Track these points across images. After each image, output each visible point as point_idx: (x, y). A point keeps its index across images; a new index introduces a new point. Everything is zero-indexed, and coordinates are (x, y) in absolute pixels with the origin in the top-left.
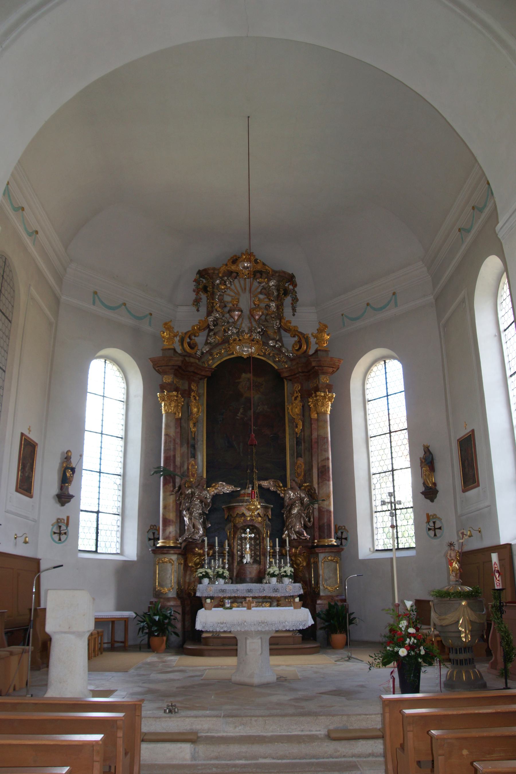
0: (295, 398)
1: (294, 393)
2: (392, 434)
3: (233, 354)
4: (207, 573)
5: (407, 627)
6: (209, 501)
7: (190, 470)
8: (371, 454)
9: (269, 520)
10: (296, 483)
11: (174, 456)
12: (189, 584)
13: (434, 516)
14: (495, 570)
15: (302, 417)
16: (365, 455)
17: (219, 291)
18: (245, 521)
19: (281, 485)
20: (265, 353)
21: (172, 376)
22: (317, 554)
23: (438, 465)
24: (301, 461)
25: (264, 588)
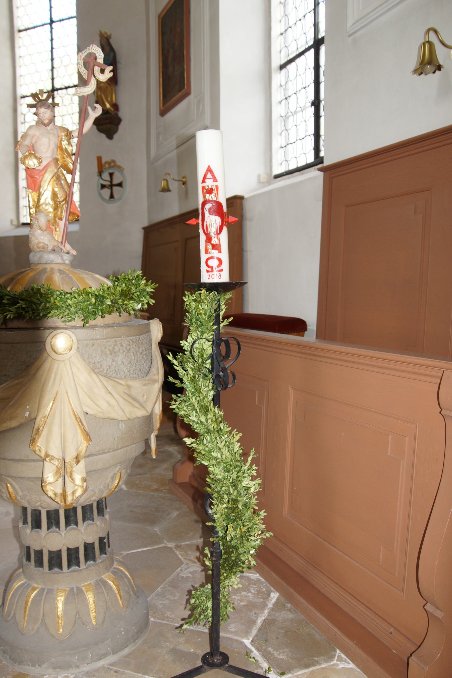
13: (112, 164)
14: (204, 203)
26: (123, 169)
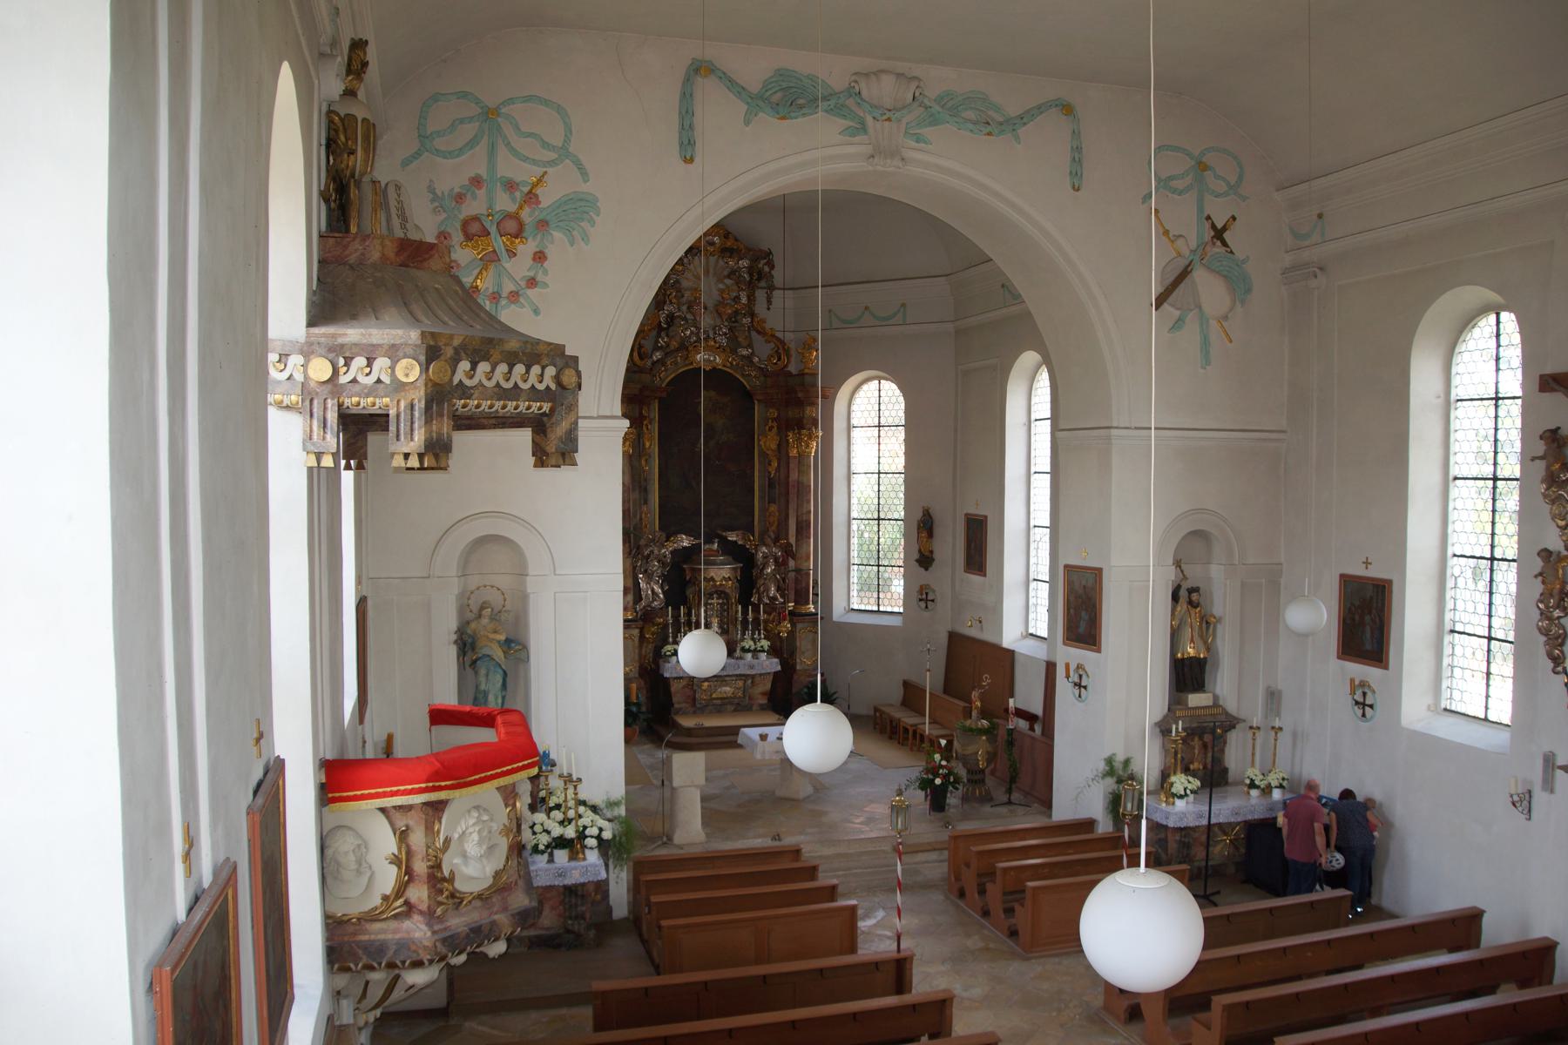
3: (692, 363)
13: (927, 586)
16: (846, 496)
18: (715, 586)
20: (731, 363)
23: (937, 531)
24: (773, 508)
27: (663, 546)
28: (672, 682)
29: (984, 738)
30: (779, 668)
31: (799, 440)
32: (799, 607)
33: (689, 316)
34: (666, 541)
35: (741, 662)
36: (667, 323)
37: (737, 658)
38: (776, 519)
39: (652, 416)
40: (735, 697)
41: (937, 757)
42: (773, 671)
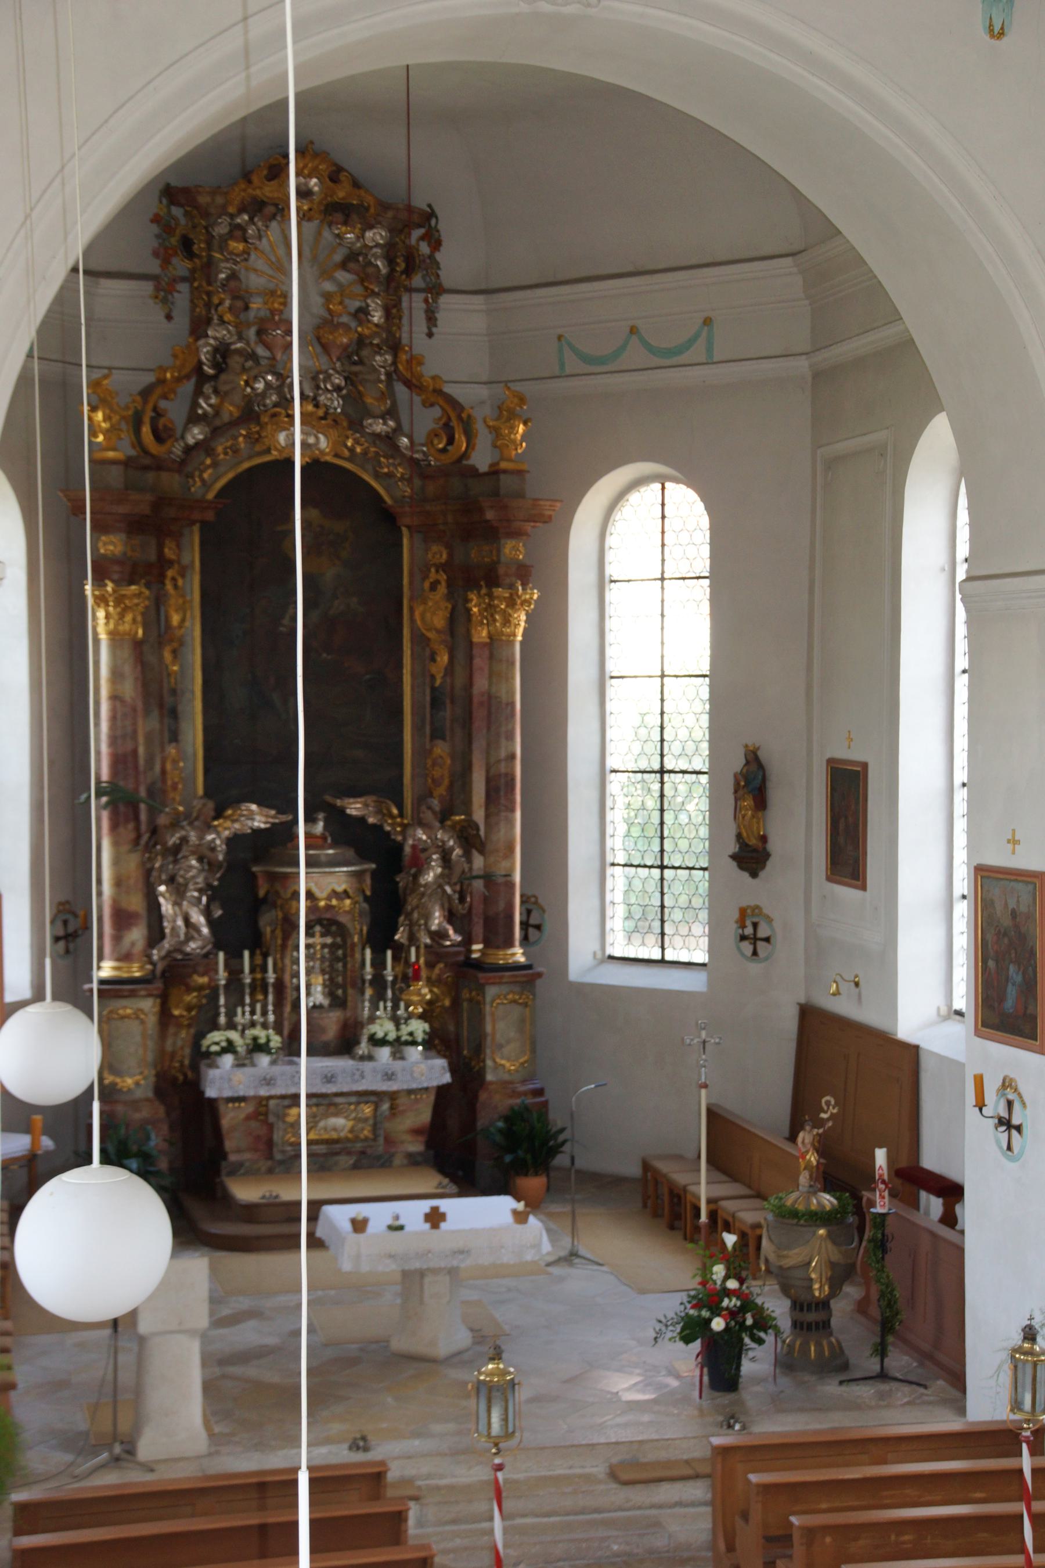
0: (431, 583)
1: (429, 570)
2: (666, 679)
3: (268, 451)
4: (230, 1042)
5: (727, 1277)
6: (221, 857)
7: (169, 776)
8: (610, 720)
9: (366, 899)
10: (434, 812)
11: (135, 752)
12: (173, 1055)
13: (757, 910)
15: (449, 639)
17: (227, 260)
19: (395, 811)
20: (352, 450)
21: (123, 536)
22: (481, 989)
23: (776, 795)
24: (441, 749)
25: (363, 1072)
26: (772, 920)
27: (208, 827)
28: (222, 1108)
29: (822, 1232)
30: (447, 1078)
31: (490, 609)
32: (490, 951)
33: (261, 351)
34: (216, 818)
35: (367, 1066)
36: (215, 365)
37: (362, 1058)
38: (446, 773)
39: (186, 560)
40: (357, 1139)
41: (719, 1271)
42: (435, 1083)
